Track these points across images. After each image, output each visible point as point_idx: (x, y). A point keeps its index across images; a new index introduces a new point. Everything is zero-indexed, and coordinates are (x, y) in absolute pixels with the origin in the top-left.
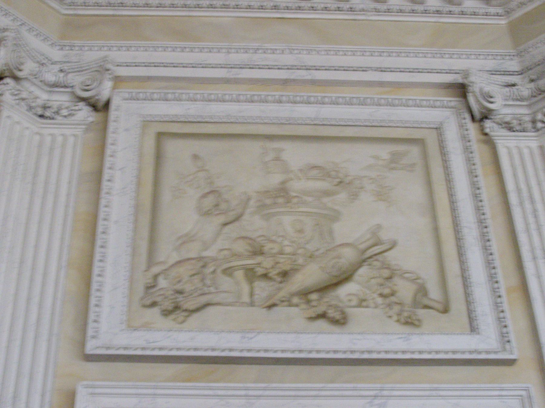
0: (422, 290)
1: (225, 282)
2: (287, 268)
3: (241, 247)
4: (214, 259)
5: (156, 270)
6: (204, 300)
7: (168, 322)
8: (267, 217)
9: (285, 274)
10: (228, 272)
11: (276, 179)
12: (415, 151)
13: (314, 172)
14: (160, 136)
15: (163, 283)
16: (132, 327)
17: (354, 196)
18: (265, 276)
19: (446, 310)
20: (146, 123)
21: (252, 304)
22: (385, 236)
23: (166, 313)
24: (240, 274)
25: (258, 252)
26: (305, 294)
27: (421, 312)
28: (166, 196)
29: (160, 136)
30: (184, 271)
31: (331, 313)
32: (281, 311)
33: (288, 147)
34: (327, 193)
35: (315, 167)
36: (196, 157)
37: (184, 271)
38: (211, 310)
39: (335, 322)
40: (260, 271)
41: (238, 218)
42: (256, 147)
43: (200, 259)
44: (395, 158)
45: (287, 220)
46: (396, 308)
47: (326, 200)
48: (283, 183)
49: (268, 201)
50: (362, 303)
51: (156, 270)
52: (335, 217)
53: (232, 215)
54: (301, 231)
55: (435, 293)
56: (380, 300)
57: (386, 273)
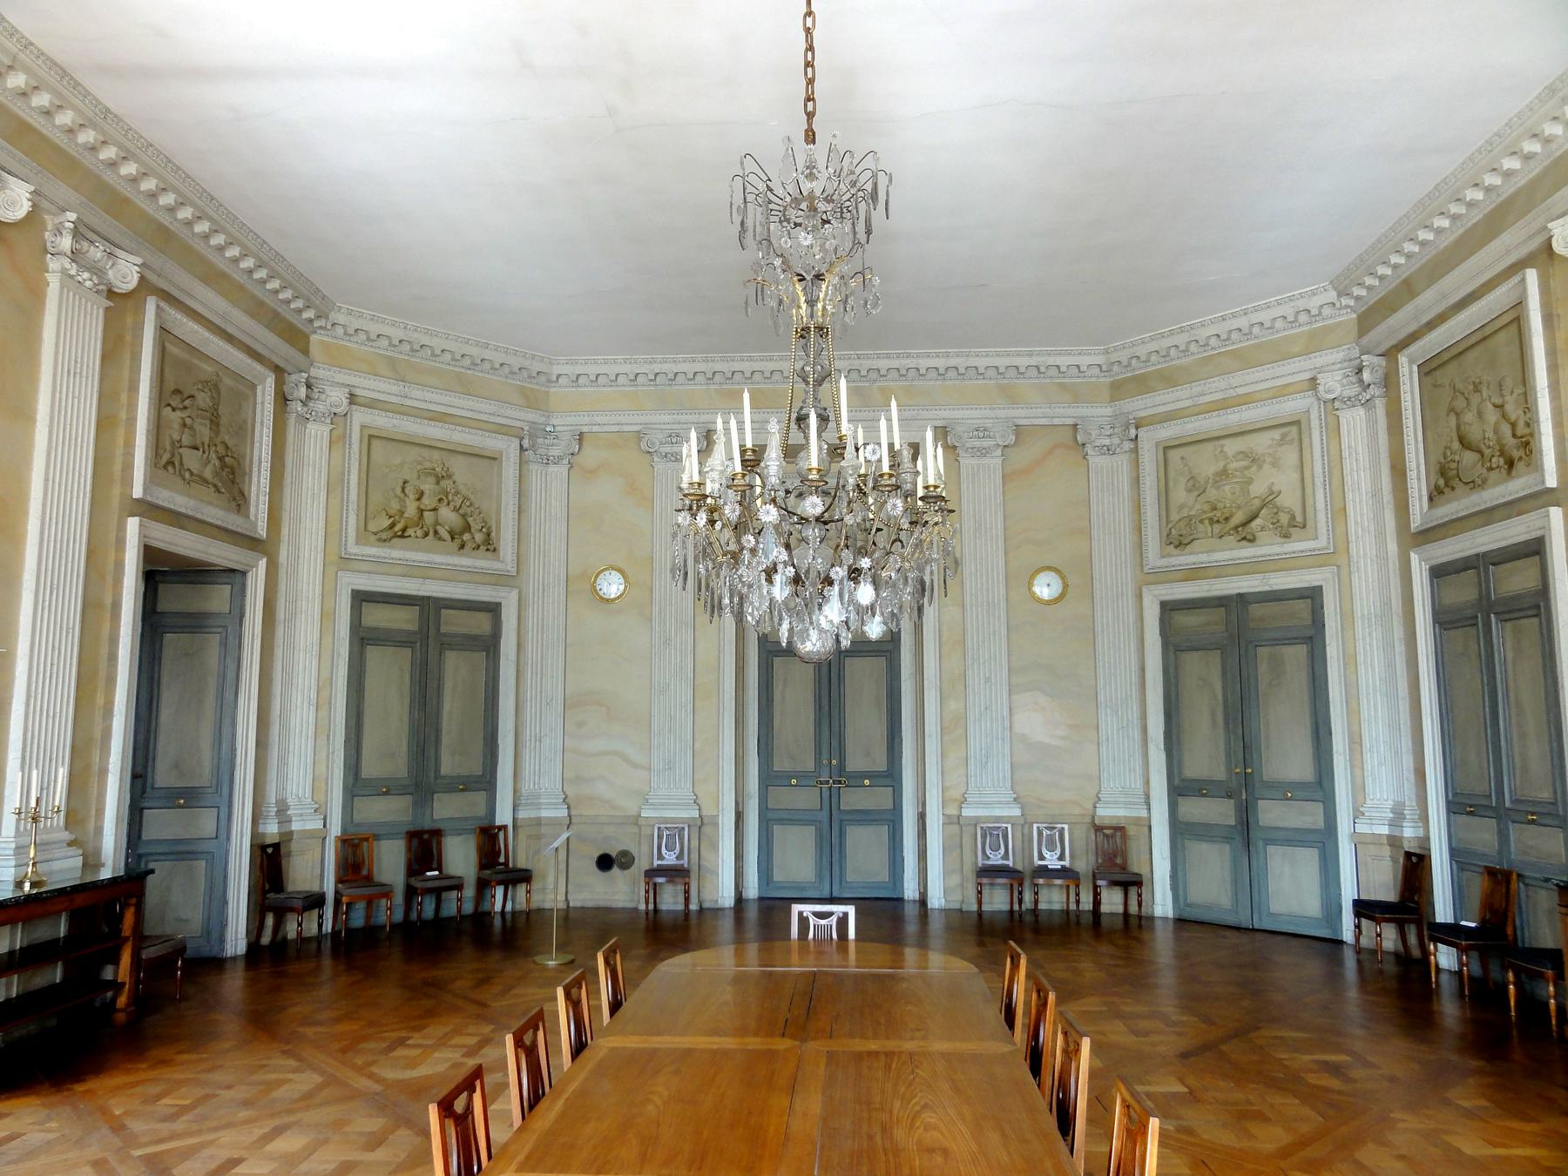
0: (1293, 517)
1: (1201, 527)
2: (1228, 515)
3: (1206, 507)
4: (1194, 516)
5: (1170, 526)
6: (1192, 537)
7: (1176, 552)
8: (1218, 488)
9: (1227, 519)
10: (1201, 521)
11: (1222, 464)
12: (1294, 429)
13: (1241, 456)
14: (1165, 448)
15: (1174, 531)
16: (1163, 557)
17: (1260, 467)
18: (1218, 521)
19: (1304, 527)
20: (1157, 444)
21: (1212, 537)
22: (1275, 489)
23: (1176, 547)
24: (1207, 522)
25: (1215, 509)
26: (1236, 528)
27: (1292, 530)
28: (1171, 484)
29: (1165, 448)
30: (1182, 524)
31: (1248, 537)
32: (1227, 538)
33: (1227, 442)
34: (1247, 468)
35: (1242, 452)
36: (1182, 458)
37: (1182, 524)
38: (1196, 542)
39: (1250, 541)
40: (1215, 519)
41: (1204, 491)
42: (1209, 447)
43: (1188, 516)
44: (1284, 436)
45: (1227, 488)
46: (1279, 529)
47: (1246, 473)
48: (1225, 466)
49: (1218, 479)
50: (1263, 529)
51: (1170, 526)
52: (1250, 481)
53: (1201, 490)
54: (1234, 493)
55: (1299, 519)
56: (1271, 526)
57: (1275, 510)
